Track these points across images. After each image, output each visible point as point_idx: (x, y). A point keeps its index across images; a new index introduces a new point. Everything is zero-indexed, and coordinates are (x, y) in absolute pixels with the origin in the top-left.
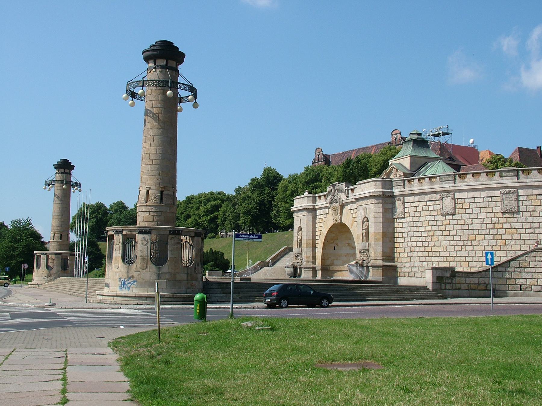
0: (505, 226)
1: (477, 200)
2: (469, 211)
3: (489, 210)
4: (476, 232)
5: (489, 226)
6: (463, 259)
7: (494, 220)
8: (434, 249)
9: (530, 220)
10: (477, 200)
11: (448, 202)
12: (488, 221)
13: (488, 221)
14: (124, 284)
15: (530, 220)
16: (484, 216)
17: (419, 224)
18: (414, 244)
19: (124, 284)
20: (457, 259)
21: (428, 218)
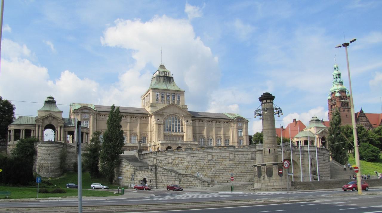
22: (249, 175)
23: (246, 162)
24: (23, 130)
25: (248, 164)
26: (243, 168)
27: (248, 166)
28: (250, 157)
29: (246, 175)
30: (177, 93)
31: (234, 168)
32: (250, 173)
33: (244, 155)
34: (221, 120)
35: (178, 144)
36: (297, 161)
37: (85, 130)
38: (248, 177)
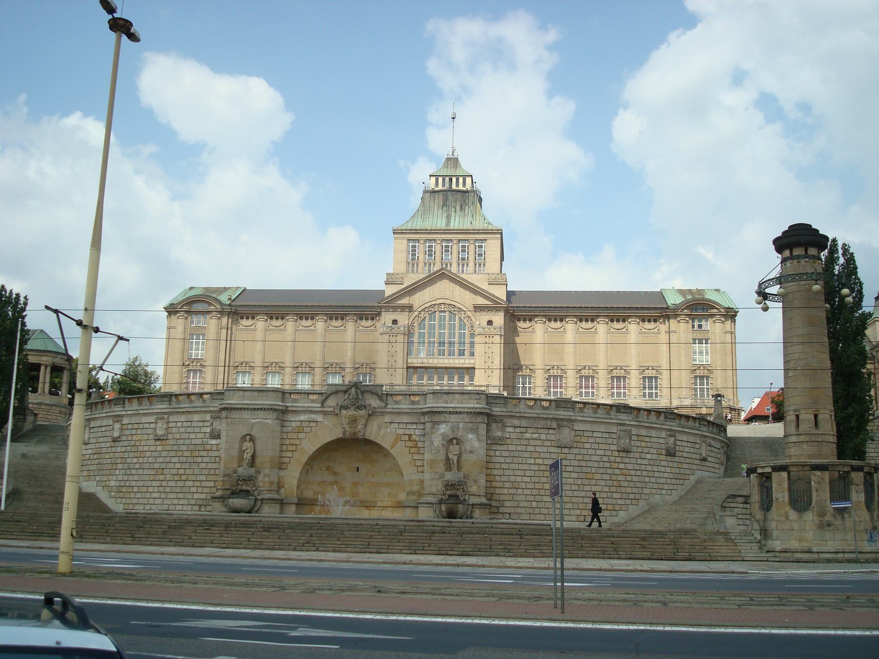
0: (622, 466)
1: (595, 434)
3: (607, 447)
4: (594, 470)
5: (607, 465)
6: (581, 500)
7: (612, 459)
9: (639, 461)
10: (595, 434)
11: (566, 434)
12: (605, 459)
13: (605, 459)
14: (871, 537)
16: (602, 452)
17: (527, 455)
18: (519, 479)
19: (871, 537)
20: (575, 500)
21: (539, 449)
22: (200, 490)
23: (198, 448)
24: (46, 367)
25: (202, 453)
26: (187, 465)
27: (199, 460)
28: (208, 430)
29: (194, 490)
31: (163, 466)
32: (204, 484)
33: (194, 424)
36: (392, 447)
37: (44, 358)
38: (196, 496)
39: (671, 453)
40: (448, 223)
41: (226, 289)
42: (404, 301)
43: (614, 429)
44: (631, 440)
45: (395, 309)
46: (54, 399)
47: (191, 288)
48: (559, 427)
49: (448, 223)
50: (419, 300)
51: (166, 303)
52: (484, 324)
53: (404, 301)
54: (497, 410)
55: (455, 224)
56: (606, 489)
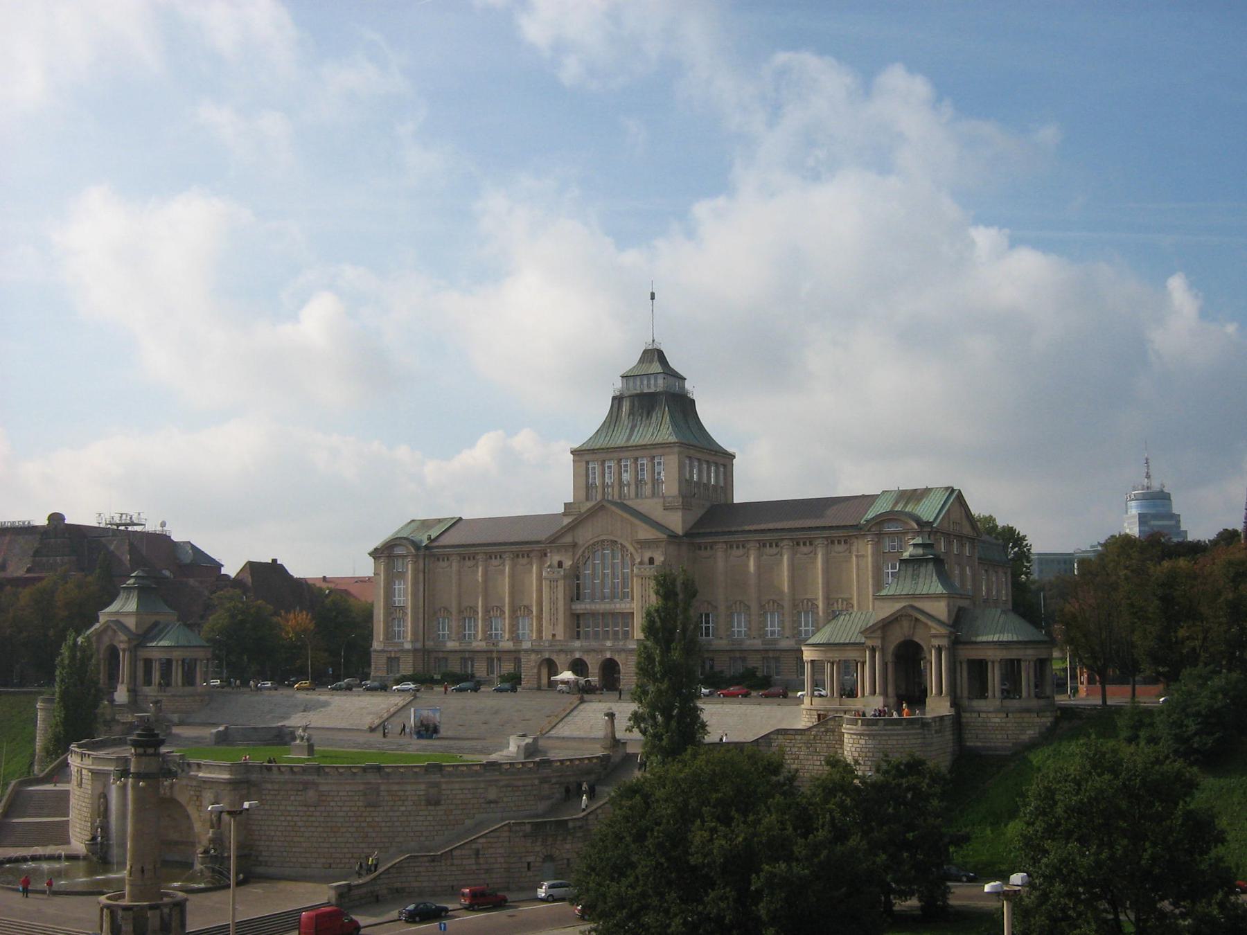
2: (332, 804)
8: (296, 839)
9: (391, 814)
15: (391, 814)
30: (654, 452)
34: (813, 534)
35: (572, 651)
39: (433, 802)
40: (628, 440)
41: (439, 521)
42: (568, 539)
43: (362, 787)
44: (378, 795)
45: (559, 549)
46: (189, 689)
47: (413, 521)
48: (305, 789)
49: (628, 440)
50: (586, 535)
51: (371, 549)
52: (646, 560)
53: (568, 539)
54: (254, 777)
55: (636, 439)
56: (352, 840)
